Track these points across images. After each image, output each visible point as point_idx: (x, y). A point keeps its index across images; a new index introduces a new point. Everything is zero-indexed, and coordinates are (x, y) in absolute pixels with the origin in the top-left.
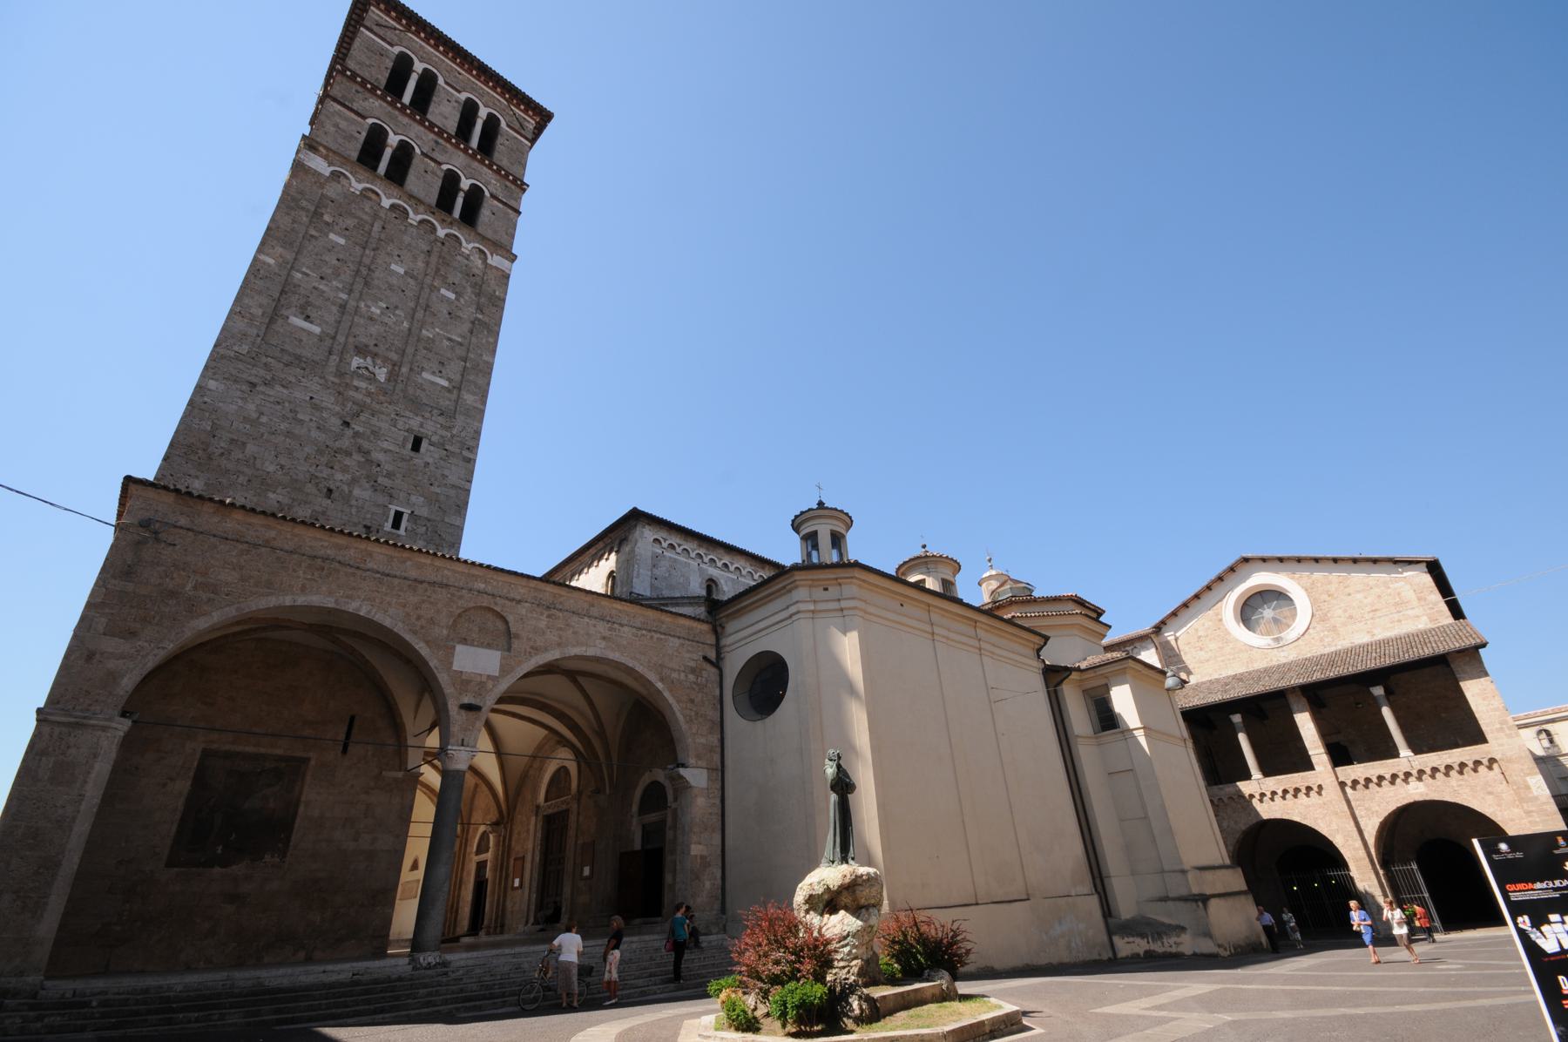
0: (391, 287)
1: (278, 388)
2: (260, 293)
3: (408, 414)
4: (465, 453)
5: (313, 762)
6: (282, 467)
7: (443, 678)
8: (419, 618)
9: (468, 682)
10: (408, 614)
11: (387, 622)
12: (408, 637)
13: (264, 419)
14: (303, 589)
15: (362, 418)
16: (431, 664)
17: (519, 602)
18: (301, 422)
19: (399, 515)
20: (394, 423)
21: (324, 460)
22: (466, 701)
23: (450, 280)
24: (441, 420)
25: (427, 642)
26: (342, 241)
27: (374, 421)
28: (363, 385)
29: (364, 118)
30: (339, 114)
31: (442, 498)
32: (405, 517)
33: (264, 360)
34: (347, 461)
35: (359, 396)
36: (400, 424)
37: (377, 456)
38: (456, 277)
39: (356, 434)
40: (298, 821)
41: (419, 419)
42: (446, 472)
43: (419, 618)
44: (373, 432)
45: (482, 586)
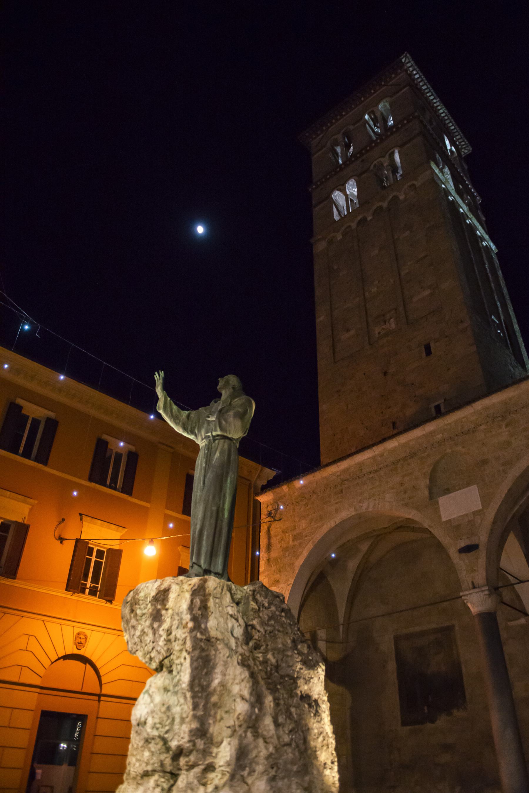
5: (457, 628)
7: (439, 533)
8: (405, 492)
9: (458, 527)
14: (337, 510)
17: (474, 430)
32: (442, 407)
40: (465, 679)
45: (439, 437)
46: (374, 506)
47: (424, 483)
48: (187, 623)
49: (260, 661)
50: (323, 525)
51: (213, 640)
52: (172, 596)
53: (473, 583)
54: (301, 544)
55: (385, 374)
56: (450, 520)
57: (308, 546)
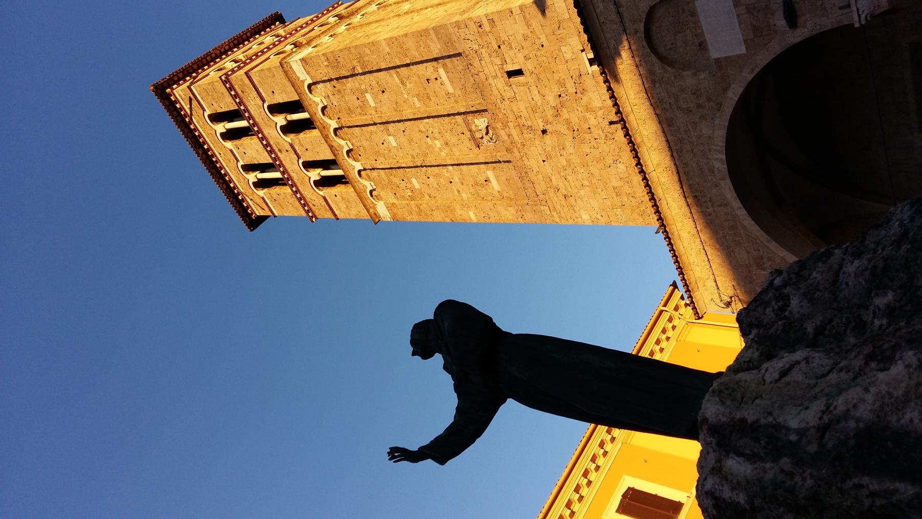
0: (410, 141)
1: (555, 182)
2: (497, 212)
3: (496, 92)
4: (487, 27)
6: (615, 161)
7: (762, 59)
8: (700, 106)
10: (703, 117)
11: (720, 135)
12: (728, 111)
13: (586, 183)
15: (530, 124)
16: (750, 77)
18: (569, 161)
19: (591, 62)
20: (513, 99)
21: (588, 136)
22: (782, 23)
23: (357, 103)
24: (476, 63)
25: (725, 90)
26: (413, 180)
27: (524, 114)
28: (502, 133)
29: (325, 198)
30: (340, 209)
31: (548, 30)
33: (541, 196)
34: (575, 120)
35: (515, 133)
36: (509, 94)
37: (552, 100)
38: (352, 99)
39: (547, 123)
41: (491, 80)
42: (520, 38)
43: (700, 106)
44: (534, 111)
46: (719, 151)
47: (689, 80)
48: (782, 471)
49: (889, 325)
50: (744, 227)
51: (826, 418)
52: (726, 493)
53: (841, 8)
54: (769, 259)
55: (544, 132)
56: (745, 41)
57: (773, 249)
